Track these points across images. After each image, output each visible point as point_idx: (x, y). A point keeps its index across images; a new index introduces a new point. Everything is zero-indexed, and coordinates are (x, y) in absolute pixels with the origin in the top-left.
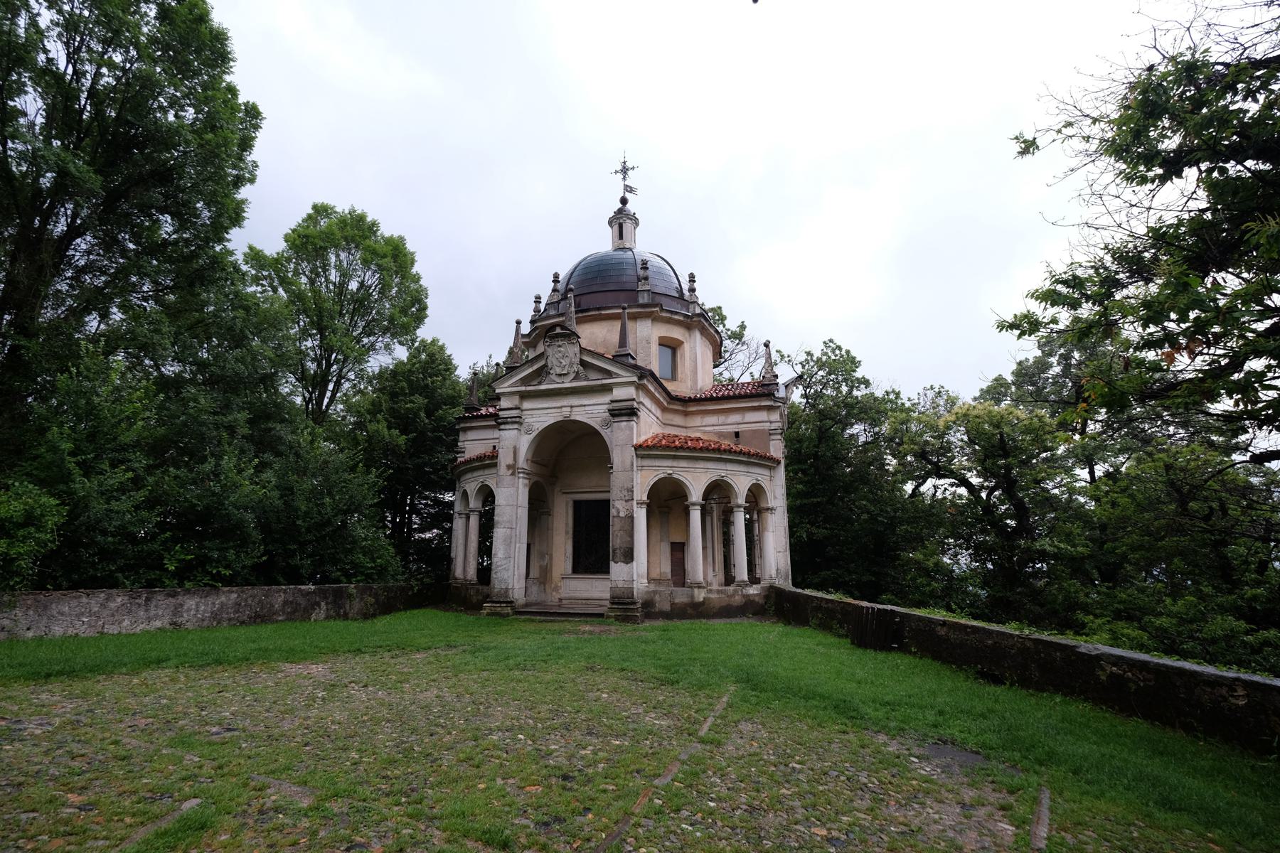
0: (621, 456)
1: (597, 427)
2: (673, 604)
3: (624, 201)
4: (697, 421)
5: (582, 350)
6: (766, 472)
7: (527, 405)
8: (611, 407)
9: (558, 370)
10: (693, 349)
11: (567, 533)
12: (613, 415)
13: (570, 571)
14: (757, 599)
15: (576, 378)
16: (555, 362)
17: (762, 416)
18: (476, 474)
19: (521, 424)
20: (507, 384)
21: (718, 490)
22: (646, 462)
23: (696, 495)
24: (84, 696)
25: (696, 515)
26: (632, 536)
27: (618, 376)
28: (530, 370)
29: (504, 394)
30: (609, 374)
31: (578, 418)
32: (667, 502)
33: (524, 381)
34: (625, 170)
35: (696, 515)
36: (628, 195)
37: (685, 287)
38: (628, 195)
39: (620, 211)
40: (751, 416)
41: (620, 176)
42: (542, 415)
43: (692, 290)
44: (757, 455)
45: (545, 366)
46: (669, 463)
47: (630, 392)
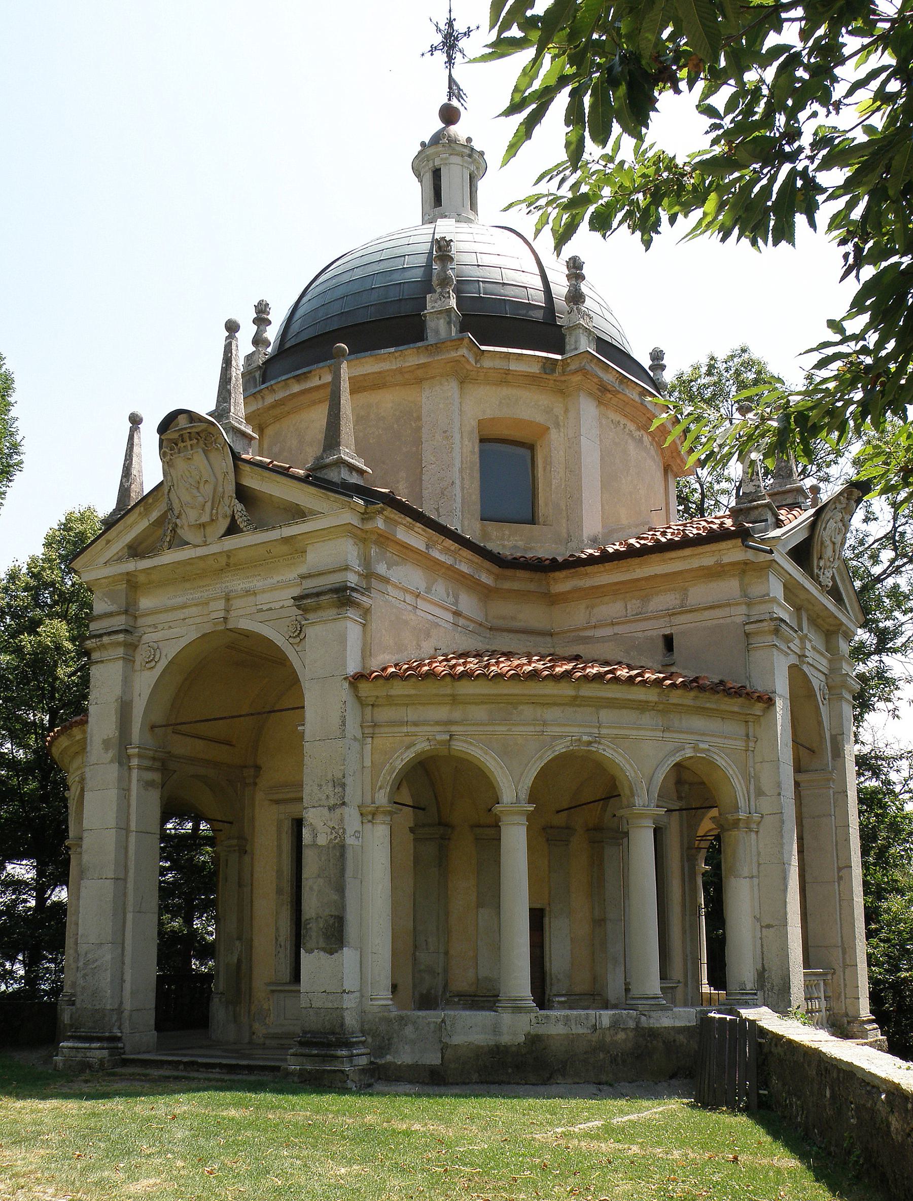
0: (324, 707)
1: (280, 641)
6: (734, 728)
8: (296, 592)
9: (192, 516)
10: (574, 444)
12: (305, 610)
14: (681, 1038)
15: (233, 529)
16: (186, 498)
17: (730, 587)
19: (131, 647)
22: (385, 714)
23: (512, 786)
25: (516, 841)
26: (341, 889)
28: (144, 524)
30: (298, 513)
31: (245, 624)
32: (440, 810)
33: (135, 551)
35: (516, 841)
37: (560, 286)
40: (700, 593)
43: (576, 297)
44: (721, 688)
46: (442, 713)
47: (348, 551)
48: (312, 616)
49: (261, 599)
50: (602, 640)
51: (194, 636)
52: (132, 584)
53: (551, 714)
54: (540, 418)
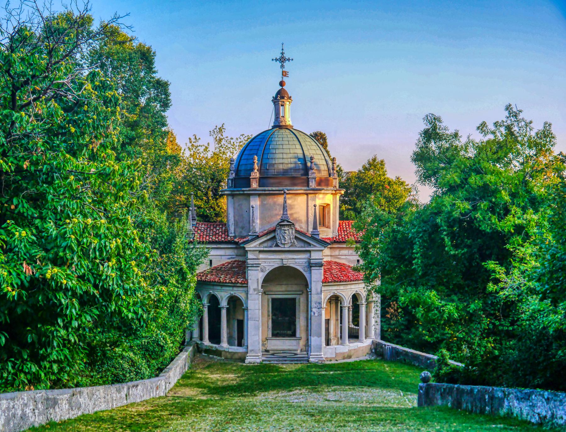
1: (302, 270)
2: (336, 354)
3: (282, 84)
4: (337, 252)
5: (297, 231)
7: (261, 256)
11: (269, 316)
13: (270, 335)
18: (228, 288)
20: (252, 246)
21: (355, 298)
24: (13, 399)
27: (315, 246)
29: (250, 251)
30: (309, 244)
31: (291, 265)
34: (282, 60)
36: (285, 79)
38: (285, 79)
39: (279, 93)
41: (278, 64)
42: (270, 262)
45: (274, 238)
48: (313, 268)
49: (296, 260)
50: (343, 259)
51: (277, 266)
52: (260, 251)
53: (353, 286)
54: (329, 203)
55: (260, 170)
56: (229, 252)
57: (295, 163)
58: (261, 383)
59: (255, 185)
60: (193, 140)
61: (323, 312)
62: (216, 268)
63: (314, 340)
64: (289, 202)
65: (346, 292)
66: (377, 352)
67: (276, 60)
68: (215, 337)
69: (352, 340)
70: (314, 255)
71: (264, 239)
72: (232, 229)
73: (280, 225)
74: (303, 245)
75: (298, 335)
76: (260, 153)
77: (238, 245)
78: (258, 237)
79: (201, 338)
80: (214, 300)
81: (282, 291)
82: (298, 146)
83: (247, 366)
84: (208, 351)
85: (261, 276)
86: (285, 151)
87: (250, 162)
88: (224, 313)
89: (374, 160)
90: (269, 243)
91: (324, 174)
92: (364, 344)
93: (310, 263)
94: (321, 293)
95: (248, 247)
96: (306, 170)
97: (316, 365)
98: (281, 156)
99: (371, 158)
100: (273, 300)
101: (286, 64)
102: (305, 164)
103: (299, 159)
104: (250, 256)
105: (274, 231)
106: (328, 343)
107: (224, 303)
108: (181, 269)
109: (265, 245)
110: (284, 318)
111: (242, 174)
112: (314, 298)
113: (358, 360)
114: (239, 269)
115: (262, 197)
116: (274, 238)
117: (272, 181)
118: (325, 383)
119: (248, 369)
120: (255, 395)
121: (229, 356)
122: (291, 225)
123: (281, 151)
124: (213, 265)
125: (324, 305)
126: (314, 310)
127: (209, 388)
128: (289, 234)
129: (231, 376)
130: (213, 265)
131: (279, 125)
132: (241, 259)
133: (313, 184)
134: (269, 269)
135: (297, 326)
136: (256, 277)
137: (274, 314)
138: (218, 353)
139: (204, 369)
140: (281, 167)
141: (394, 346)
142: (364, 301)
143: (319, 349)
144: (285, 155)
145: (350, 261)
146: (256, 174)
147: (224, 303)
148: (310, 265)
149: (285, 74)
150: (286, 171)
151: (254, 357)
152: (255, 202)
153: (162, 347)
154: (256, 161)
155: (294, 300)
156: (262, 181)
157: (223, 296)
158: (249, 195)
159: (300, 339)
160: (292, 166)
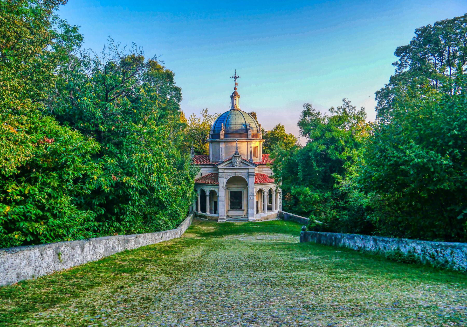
3: (235, 89)
4: (261, 169)
5: (242, 159)
7: (225, 171)
21: (270, 191)
24: (108, 240)
30: (248, 165)
34: (235, 77)
36: (237, 87)
38: (237, 87)
39: (234, 93)
42: (230, 174)
45: (232, 162)
46: (260, 186)
52: (225, 169)
53: (269, 185)
55: (225, 130)
56: (210, 169)
57: (242, 127)
58: (226, 231)
59: (222, 137)
60: (193, 116)
61: (255, 197)
62: (204, 177)
63: (251, 211)
64: (238, 145)
65: (266, 188)
66: (280, 216)
67: (232, 77)
68: (204, 209)
69: (269, 211)
70: (251, 171)
71: (227, 163)
72: (211, 158)
73: (234, 156)
74: (245, 165)
75: (243, 209)
76: (225, 122)
77: (215, 166)
78: (224, 162)
79: (197, 210)
80: (203, 192)
81: (235, 188)
82: (243, 119)
83: (219, 223)
84: (201, 216)
85: (225, 180)
86: (237, 121)
87: (220, 126)
88: (208, 198)
89: (279, 125)
90: (229, 165)
91: (255, 132)
92: (275, 212)
93: (248, 174)
94: (254, 188)
95: (219, 167)
96: (247, 130)
97: (251, 223)
98: (235, 123)
99: (277, 124)
100: (231, 192)
101: (237, 79)
102: (246, 127)
103: (243, 125)
104: (220, 171)
105: (231, 159)
106: (257, 212)
107: (208, 194)
108: (188, 177)
109: (227, 166)
110: (236, 200)
111: (216, 132)
112: (250, 191)
113: (271, 220)
114: (215, 177)
115: (226, 143)
116: (232, 162)
117: (230, 135)
118: (256, 231)
119: (219, 224)
120: (223, 237)
121: (210, 218)
122: (240, 156)
123: (235, 121)
124: (203, 175)
125: (255, 194)
126: (250, 196)
127: (201, 234)
128: (238, 160)
129: (211, 228)
130: (203, 175)
131: (234, 109)
132: (216, 172)
133: (250, 137)
134: (229, 177)
135: (243, 204)
136: (223, 181)
137: (231, 198)
138: (205, 217)
139: (198, 224)
140: (235, 129)
141: (289, 213)
142: (274, 193)
143: (253, 215)
144: (237, 123)
145: (267, 173)
146: (223, 132)
147: (208, 194)
148: (249, 175)
149: (236, 84)
150: (237, 131)
151: (222, 219)
152: (222, 146)
153: (179, 214)
154: (223, 126)
155: (241, 192)
156: (226, 135)
157: (207, 190)
158: (220, 142)
159: (244, 210)
160: (240, 128)
